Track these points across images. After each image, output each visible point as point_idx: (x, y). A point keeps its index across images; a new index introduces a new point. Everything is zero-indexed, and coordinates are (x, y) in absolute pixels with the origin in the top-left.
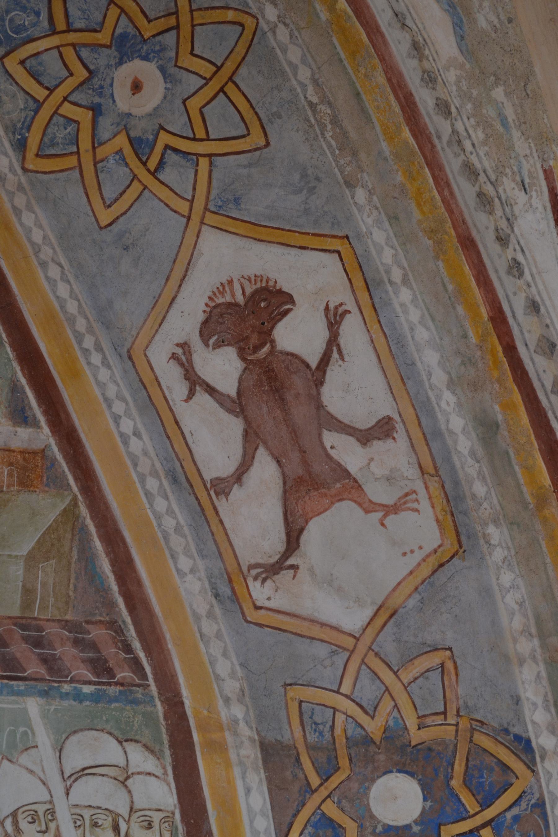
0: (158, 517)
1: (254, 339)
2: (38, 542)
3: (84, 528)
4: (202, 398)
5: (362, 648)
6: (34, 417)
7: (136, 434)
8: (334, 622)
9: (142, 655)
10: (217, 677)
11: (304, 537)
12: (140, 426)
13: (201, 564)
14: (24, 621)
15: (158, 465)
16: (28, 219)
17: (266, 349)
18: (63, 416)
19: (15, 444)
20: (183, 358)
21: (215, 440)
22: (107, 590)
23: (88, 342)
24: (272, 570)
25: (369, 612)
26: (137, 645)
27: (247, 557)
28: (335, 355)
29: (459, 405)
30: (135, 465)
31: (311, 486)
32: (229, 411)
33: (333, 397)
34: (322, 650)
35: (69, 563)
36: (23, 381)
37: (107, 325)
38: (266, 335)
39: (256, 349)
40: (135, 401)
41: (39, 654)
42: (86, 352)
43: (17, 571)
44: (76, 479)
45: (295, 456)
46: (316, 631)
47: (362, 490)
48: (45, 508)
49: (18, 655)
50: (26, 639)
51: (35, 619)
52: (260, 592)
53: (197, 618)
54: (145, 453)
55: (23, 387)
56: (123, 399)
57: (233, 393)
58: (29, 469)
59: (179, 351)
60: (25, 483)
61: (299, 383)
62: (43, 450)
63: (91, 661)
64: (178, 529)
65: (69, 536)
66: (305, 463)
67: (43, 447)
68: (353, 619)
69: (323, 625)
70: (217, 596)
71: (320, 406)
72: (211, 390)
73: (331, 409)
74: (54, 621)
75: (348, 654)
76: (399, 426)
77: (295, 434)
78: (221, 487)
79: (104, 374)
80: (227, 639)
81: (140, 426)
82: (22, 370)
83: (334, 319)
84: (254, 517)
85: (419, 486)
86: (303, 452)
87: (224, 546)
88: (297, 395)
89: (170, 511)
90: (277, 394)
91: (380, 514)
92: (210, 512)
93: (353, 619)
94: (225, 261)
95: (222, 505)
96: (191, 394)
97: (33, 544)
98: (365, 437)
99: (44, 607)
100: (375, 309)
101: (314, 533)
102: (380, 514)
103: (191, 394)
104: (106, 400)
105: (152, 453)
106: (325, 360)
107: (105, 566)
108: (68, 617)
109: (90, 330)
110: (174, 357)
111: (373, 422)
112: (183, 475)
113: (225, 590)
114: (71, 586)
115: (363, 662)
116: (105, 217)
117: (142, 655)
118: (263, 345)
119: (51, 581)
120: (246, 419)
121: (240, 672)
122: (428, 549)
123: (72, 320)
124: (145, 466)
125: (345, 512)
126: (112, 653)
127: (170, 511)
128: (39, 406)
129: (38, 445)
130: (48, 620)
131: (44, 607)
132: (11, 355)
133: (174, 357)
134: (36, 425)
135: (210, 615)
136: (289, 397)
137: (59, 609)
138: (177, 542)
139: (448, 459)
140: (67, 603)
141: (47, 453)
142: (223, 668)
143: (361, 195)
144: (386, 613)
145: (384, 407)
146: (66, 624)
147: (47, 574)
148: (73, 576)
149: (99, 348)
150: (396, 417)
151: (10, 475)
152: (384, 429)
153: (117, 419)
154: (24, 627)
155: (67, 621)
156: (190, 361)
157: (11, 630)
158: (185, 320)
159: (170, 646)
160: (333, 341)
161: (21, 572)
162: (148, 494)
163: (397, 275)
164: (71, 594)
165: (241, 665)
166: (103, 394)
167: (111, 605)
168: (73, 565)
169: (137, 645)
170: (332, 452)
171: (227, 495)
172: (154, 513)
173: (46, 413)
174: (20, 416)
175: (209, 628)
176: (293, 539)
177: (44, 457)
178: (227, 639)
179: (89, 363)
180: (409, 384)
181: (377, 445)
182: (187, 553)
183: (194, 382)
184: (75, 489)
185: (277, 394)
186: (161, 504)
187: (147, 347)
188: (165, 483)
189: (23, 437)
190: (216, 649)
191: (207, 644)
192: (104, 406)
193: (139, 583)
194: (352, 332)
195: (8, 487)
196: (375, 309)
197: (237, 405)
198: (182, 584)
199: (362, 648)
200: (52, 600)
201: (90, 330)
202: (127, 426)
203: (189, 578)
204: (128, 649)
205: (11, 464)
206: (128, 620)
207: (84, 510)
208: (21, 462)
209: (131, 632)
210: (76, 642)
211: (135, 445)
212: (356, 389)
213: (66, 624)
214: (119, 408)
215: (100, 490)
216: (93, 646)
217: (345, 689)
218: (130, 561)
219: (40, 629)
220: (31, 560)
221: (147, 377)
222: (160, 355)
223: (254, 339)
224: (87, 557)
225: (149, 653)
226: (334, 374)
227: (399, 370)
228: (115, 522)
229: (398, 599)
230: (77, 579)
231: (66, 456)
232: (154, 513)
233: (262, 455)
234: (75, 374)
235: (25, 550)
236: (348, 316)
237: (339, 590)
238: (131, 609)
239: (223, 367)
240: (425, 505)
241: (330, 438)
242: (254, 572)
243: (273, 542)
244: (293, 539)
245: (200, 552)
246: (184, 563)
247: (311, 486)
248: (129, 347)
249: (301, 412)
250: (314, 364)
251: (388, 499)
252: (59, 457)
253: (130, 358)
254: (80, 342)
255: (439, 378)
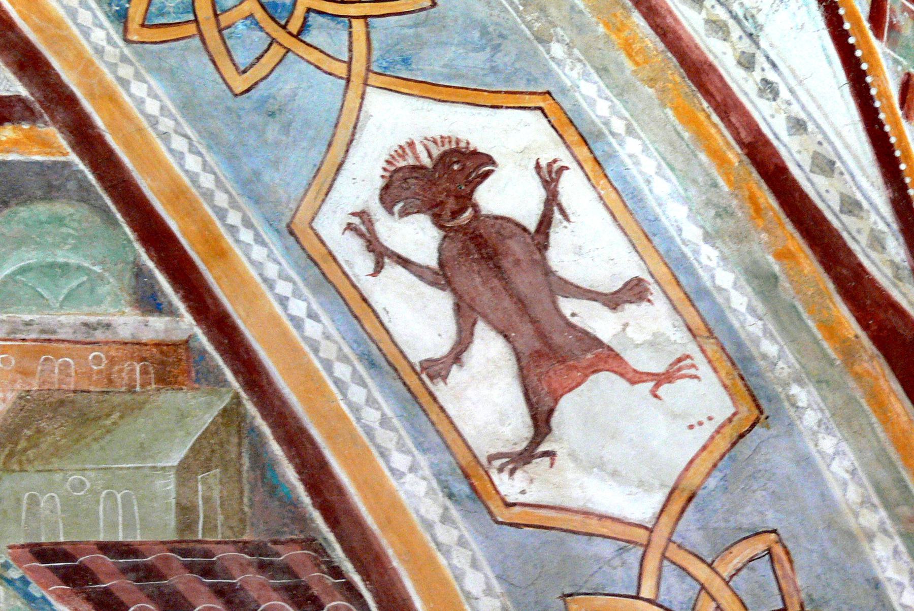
0: (356, 409)
1: (451, 204)
2: (192, 449)
3: (254, 430)
4: (393, 271)
5: (659, 539)
6: (170, 304)
7: (312, 316)
8: (615, 512)
9: (357, 579)
10: (468, 595)
11: (555, 420)
12: (315, 307)
13: (423, 460)
14: (184, 546)
15: (347, 350)
16: (139, 89)
17: (468, 213)
18: (209, 301)
19: (147, 336)
20: (362, 228)
21: (419, 318)
22: (295, 504)
23: (234, 218)
24: (522, 458)
25: (658, 498)
26: (348, 567)
27: (483, 450)
28: (557, 216)
29: (724, 258)
30: (316, 351)
31: (554, 361)
32: (434, 284)
33: (562, 256)
34: (606, 549)
35: (240, 472)
36: (151, 265)
37: (257, 200)
38: (465, 200)
39: (455, 214)
40: (305, 280)
41: (211, 585)
42: (232, 229)
43: (168, 486)
44: (236, 373)
45: (527, 329)
46: (594, 525)
47: (621, 358)
48: (196, 410)
49: (181, 587)
50: (189, 567)
51: (199, 541)
52: (511, 486)
53: (429, 525)
54: (328, 337)
55: (150, 271)
56: (288, 279)
57: (433, 263)
58: (168, 365)
59: (356, 221)
60: (166, 379)
61: (516, 247)
62: (187, 341)
63: (286, 588)
64: (384, 422)
65: (235, 440)
66: (541, 334)
67: (185, 337)
68: (641, 507)
69: (602, 517)
70: (450, 496)
71: (548, 272)
72: (404, 262)
73: (562, 273)
74: (226, 543)
75: (640, 551)
76: (653, 288)
77: (522, 304)
78: (436, 369)
79: (258, 253)
80: (474, 545)
81: (315, 307)
82: (148, 251)
83: (549, 177)
84: (486, 397)
85: (692, 348)
86: (534, 321)
87: (451, 436)
88: (517, 262)
89: (371, 401)
90: (490, 263)
91: (650, 385)
92: (425, 399)
93: (641, 507)
94: (397, 124)
95: (441, 390)
96: (379, 267)
97: (184, 452)
98: (613, 301)
99: (210, 527)
100: (598, 167)
101: (569, 411)
102: (650, 385)
103: (379, 267)
104: (265, 280)
105: (338, 337)
106: (545, 222)
107: (290, 473)
108: (245, 538)
109: (234, 205)
110: (350, 227)
111: (619, 285)
112: (382, 356)
113: (462, 488)
114: (246, 500)
115: (664, 557)
116: (240, 84)
117: (357, 579)
118: (463, 210)
119: (216, 495)
120: (454, 291)
121: (498, 588)
122: (720, 419)
123: (209, 196)
124: (328, 350)
125: (605, 383)
126: (315, 579)
127: (371, 401)
128: (176, 292)
129: (178, 336)
130: (219, 543)
131: (210, 527)
132: (131, 235)
133: (350, 227)
134: (172, 312)
135: (446, 519)
136: (507, 263)
137: (231, 528)
138: (385, 437)
139: (722, 318)
140: (242, 521)
141: (192, 344)
142: (474, 582)
143: (557, 50)
144: (682, 497)
145: (630, 267)
146: (243, 546)
147: (209, 487)
148: (247, 488)
149: (248, 224)
150: (648, 278)
151: (144, 372)
152: (634, 292)
153: (283, 301)
154: (185, 553)
155: (245, 542)
156: (372, 231)
157: (167, 558)
158: (360, 183)
159: (395, 563)
160: (552, 200)
161: (172, 487)
162: (337, 382)
163: (618, 126)
164: (246, 509)
165: (499, 577)
166: (261, 275)
167: (302, 520)
168: (245, 475)
169: (348, 567)
170: (574, 320)
171: (444, 378)
172: (350, 404)
173: (186, 299)
174: (150, 303)
175: (446, 535)
176: (542, 422)
177: (188, 349)
178: (474, 545)
179: (237, 241)
180: (656, 240)
181: (631, 309)
182: (402, 448)
183: (381, 255)
184: (236, 385)
185: (490, 263)
186: (357, 394)
187: (313, 219)
188: (360, 368)
189: (157, 327)
190: (460, 559)
191: (447, 554)
192: (264, 287)
193: (340, 490)
194: (574, 188)
195: (142, 386)
196: (598, 167)
197: (441, 276)
198: (403, 486)
199: (659, 539)
200: (221, 518)
201: (234, 205)
202: (298, 308)
203: (410, 477)
204: (336, 572)
205: (144, 359)
206: (331, 537)
207: (251, 408)
208: (158, 356)
209: (338, 553)
210: (262, 567)
211: (312, 329)
212: (590, 248)
213: (243, 546)
214: (284, 288)
215: (270, 382)
216: (287, 570)
217: (646, 592)
218: (323, 465)
219: (207, 554)
220: (185, 470)
221: (317, 252)
222: (331, 225)
223: (451, 204)
224: (261, 462)
225: (366, 577)
226: (559, 236)
227: (640, 228)
228: (296, 419)
229: (693, 480)
230: (252, 491)
231: (219, 347)
232: (350, 404)
233: (482, 330)
234: (218, 252)
235: (175, 459)
236: (566, 172)
237: (614, 474)
238: (333, 521)
239: (417, 237)
240: (704, 369)
241: (567, 306)
242: (497, 463)
243: (516, 427)
244: (542, 422)
245: (419, 445)
246: (400, 461)
247: (554, 361)
248: (288, 221)
249: (525, 281)
250: (532, 227)
251: (658, 367)
252: (210, 348)
253: (292, 233)
254: (223, 218)
255: (693, 233)
